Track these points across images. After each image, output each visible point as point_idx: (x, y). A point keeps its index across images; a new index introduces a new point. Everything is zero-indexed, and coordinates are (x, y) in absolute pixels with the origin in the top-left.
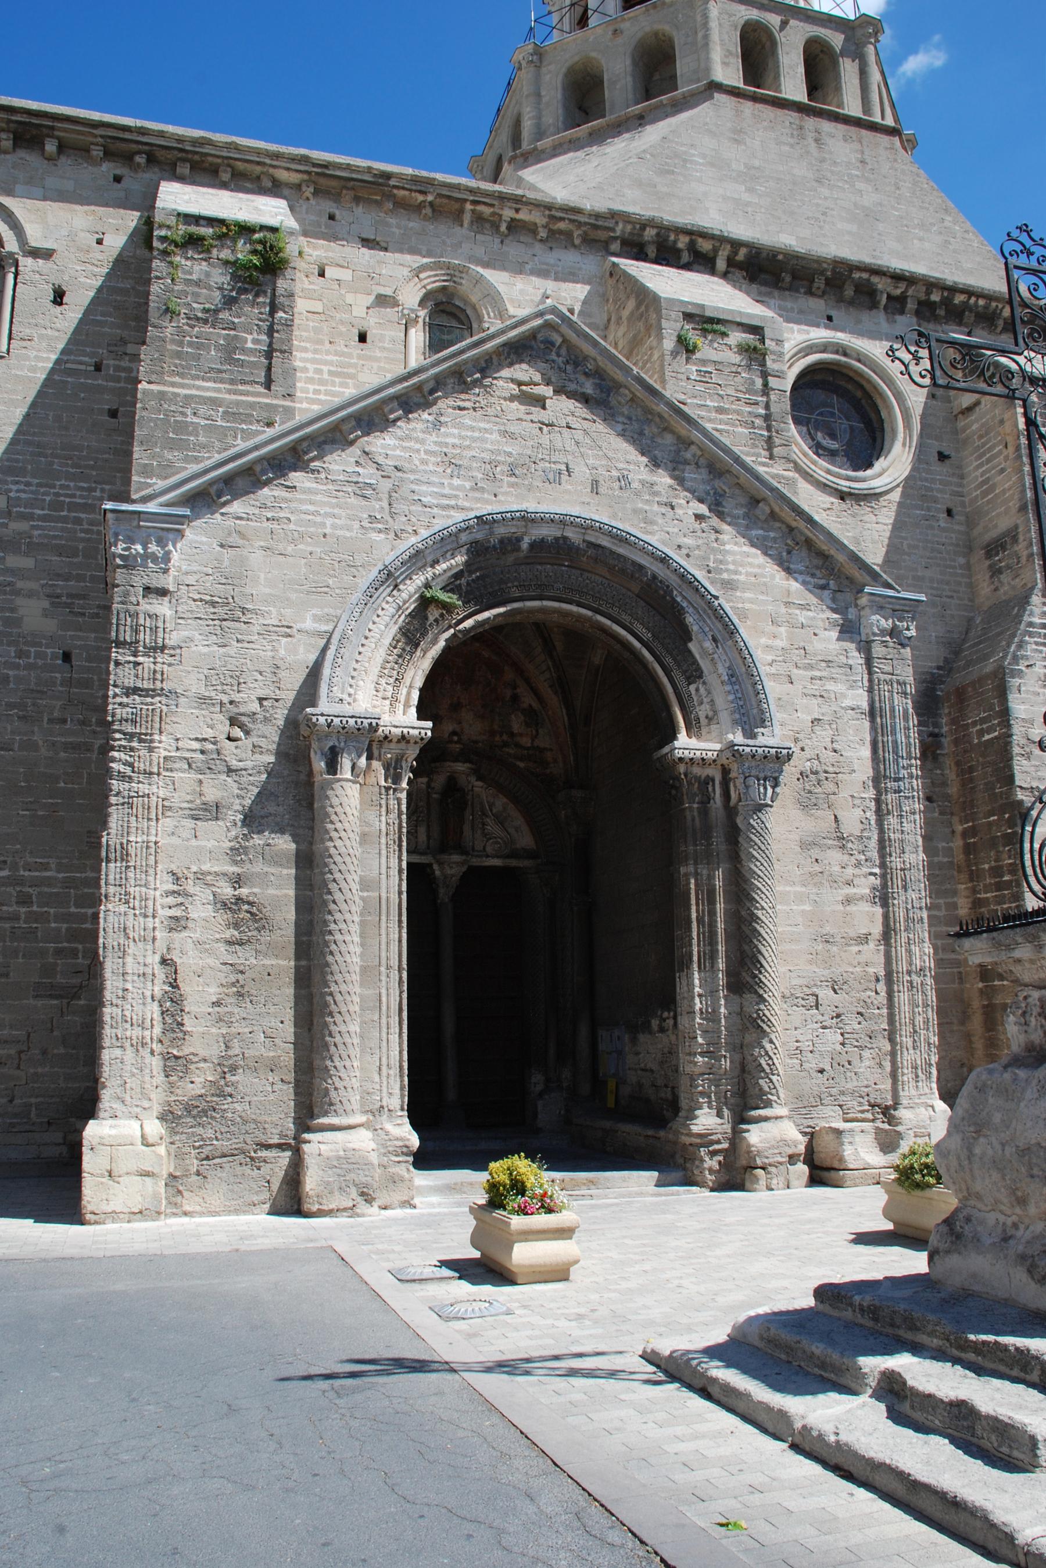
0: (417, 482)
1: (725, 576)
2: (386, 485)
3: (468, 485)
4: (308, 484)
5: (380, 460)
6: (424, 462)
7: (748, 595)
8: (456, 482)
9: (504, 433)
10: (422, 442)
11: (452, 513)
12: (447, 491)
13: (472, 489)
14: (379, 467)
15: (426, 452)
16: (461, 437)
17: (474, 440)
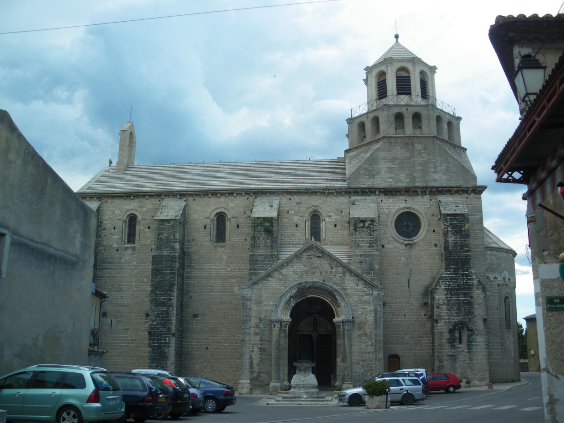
0: (289, 277)
1: (345, 288)
2: (284, 278)
3: (298, 276)
4: (271, 279)
5: (283, 274)
6: (290, 273)
7: (349, 291)
8: (296, 276)
9: (304, 266)
10: (290, 270)
11: (296, 282)
12: (294, 278)
13: (299, 277)
14: (283, 275)
15: (291, 271)
16: (297, 268)
17: (299, 268)
